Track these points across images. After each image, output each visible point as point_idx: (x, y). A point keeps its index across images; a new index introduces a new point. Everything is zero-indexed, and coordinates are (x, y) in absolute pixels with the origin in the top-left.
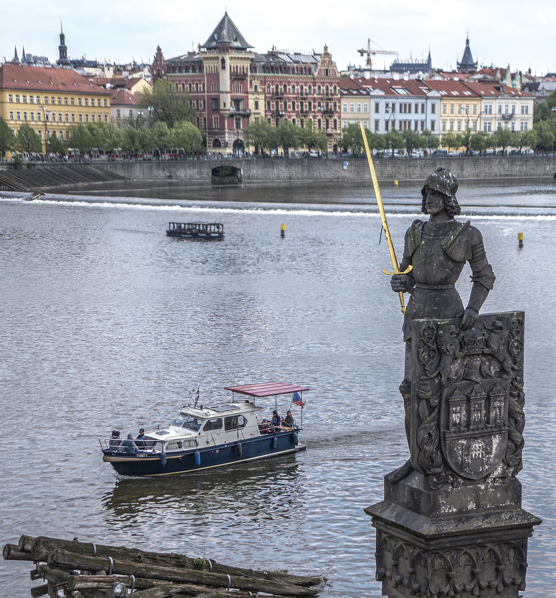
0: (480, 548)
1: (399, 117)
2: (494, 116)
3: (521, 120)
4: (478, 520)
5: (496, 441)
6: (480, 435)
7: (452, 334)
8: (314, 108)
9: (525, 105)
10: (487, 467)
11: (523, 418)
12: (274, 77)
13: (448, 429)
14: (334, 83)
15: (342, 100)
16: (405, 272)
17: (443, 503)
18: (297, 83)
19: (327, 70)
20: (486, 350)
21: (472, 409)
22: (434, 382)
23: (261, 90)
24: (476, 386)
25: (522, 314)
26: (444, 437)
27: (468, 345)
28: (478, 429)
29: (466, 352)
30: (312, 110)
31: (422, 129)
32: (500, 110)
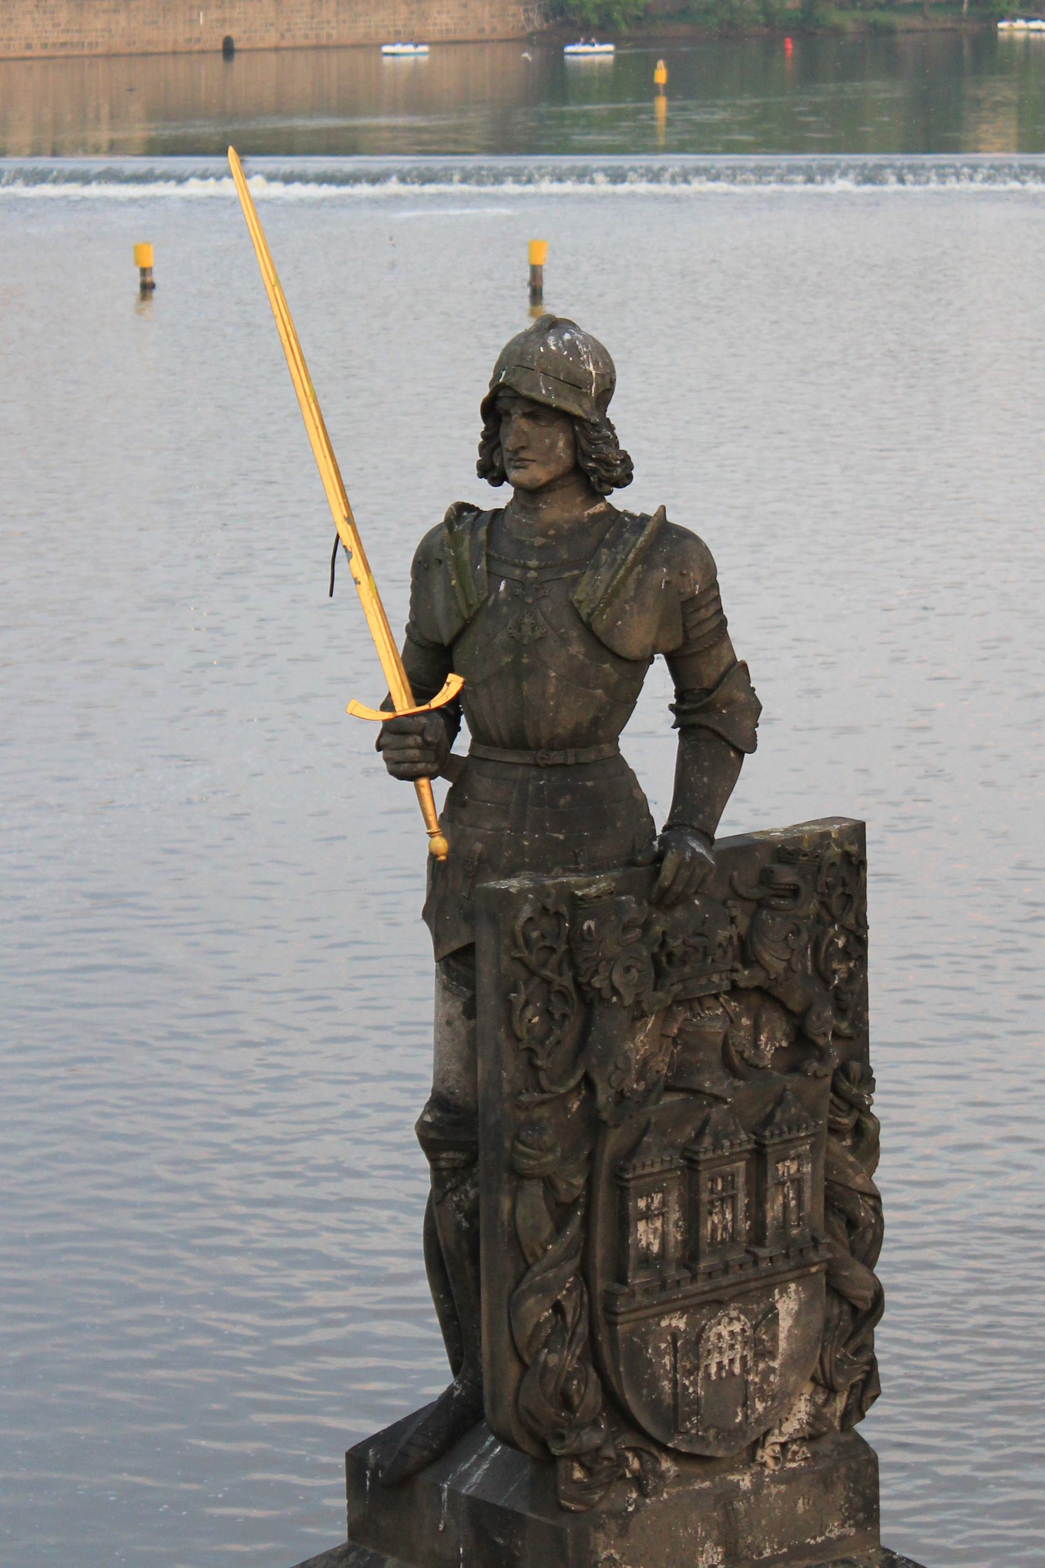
6: (732, 1291)
7: (626, 928)
10: (760, 1406)
11: (877, 1210)
13: (622, 1279)
16: (439, 700)
17: (610, 1558)
20: (745, 976)
21: (705, 1196)
22: (567, 1110)
24: (716, 1113)
25: (858, 830)
26: (610, 1312)
27: (684, 963)
28: (726, 1269)
29: (677, 988)
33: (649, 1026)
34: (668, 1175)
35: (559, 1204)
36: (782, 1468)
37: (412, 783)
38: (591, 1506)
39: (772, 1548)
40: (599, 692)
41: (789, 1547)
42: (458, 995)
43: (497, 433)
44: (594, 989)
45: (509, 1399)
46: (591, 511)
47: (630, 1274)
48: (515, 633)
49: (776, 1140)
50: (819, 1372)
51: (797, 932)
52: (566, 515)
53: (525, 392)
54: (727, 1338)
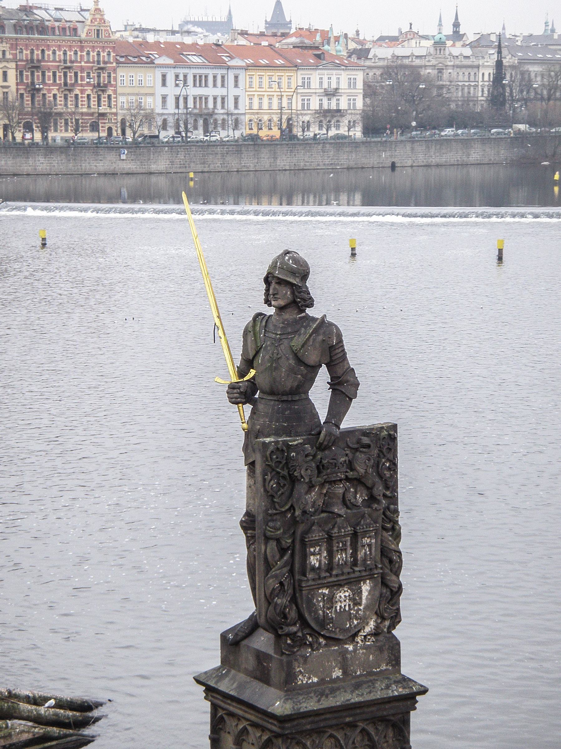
0: (349, 729)
1: (193, 91)
2: (314, 91)
3: (348, 96)
4: (345, 691)
5: (366, 588)
6: (345, 582)
7: (307, 456)
8: (81, 81)
9: (352, 77)
10: (355, 622)
11: (400, 557)
12: (28, 39)
13: (305, 575)
14: (107, 47)
15: (118, 70)
17: (300, 671)
18: (59, 47)
19: (98, 30)
20: (351, 474)
21: (335, 549)
22: (286, 517)
23: (11, 57)
24: (339, 520)
26: (300, 586)
27: (328, 468)
28: (343, 574)
30: (79, 82)
31: (223, 107)
32: (321, 83)
36: (364, 644)
38: (294, 653)
41: (367, 672)
45: (264, 614)
49: (362, 531)
51: (369, 460)
52: (291, 317)
54: (343, 597)
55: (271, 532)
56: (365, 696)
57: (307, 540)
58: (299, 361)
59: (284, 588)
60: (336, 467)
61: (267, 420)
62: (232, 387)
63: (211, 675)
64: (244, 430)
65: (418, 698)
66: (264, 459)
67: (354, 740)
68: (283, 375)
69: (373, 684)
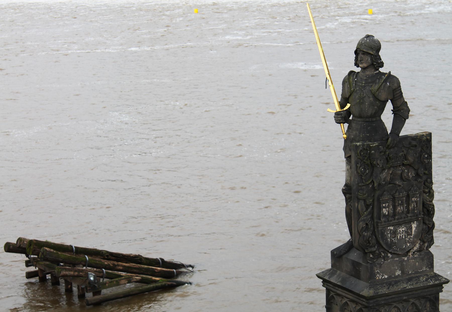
0: (405, 303)
4: (403, 283)
5: (414, 226)
7: (380, 152)
10: (408, 245)
13: (380, 220)
16: (345, 109)
17: (378, 272)
21: (397, 204)
22: (369, 187)
26: (377, 225)
27: (393, 159)
28: (401, 218)
29: (391, 164)
33: (386, 171)
34: (389, 200)
35: (367, 205)
36: (413, 256)
37: (340, 124)
38: (374, 262)
39: (411, 271)
40: (376, 107)
41: (415, 272)
42: (349, 165)
43: (358, 57)
44: (374, 164)
45: (357, 241)
46: (375, 72)
47: (381, 218)
48: (360, 96)
49: (412, 194)
50: (421, 238)
51: (416, 154)
52: (371, 73)
53: (362, 50)
54: (402, 231)
55: (361, 195)
56: (414, 285)
57: (381, 200)
58: (376, 98)
59: (368, 226)
60: (397, 158)
61: (357, 132)
62: (337, 114)
63: (326, 273)
64: (344, 138)
65: (443, 285)
66: (357, 155)
67: (408, 309)
68: (367, 107)
69: (419, 278)
